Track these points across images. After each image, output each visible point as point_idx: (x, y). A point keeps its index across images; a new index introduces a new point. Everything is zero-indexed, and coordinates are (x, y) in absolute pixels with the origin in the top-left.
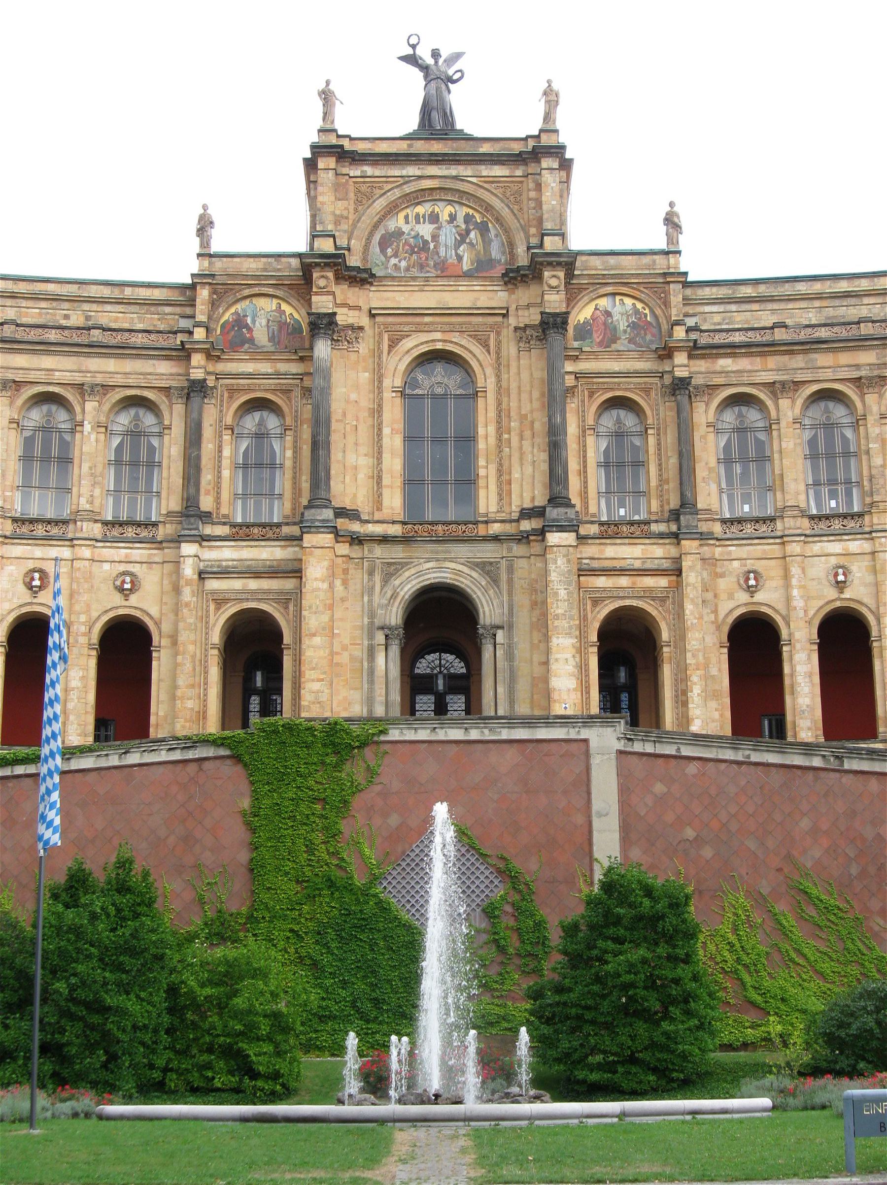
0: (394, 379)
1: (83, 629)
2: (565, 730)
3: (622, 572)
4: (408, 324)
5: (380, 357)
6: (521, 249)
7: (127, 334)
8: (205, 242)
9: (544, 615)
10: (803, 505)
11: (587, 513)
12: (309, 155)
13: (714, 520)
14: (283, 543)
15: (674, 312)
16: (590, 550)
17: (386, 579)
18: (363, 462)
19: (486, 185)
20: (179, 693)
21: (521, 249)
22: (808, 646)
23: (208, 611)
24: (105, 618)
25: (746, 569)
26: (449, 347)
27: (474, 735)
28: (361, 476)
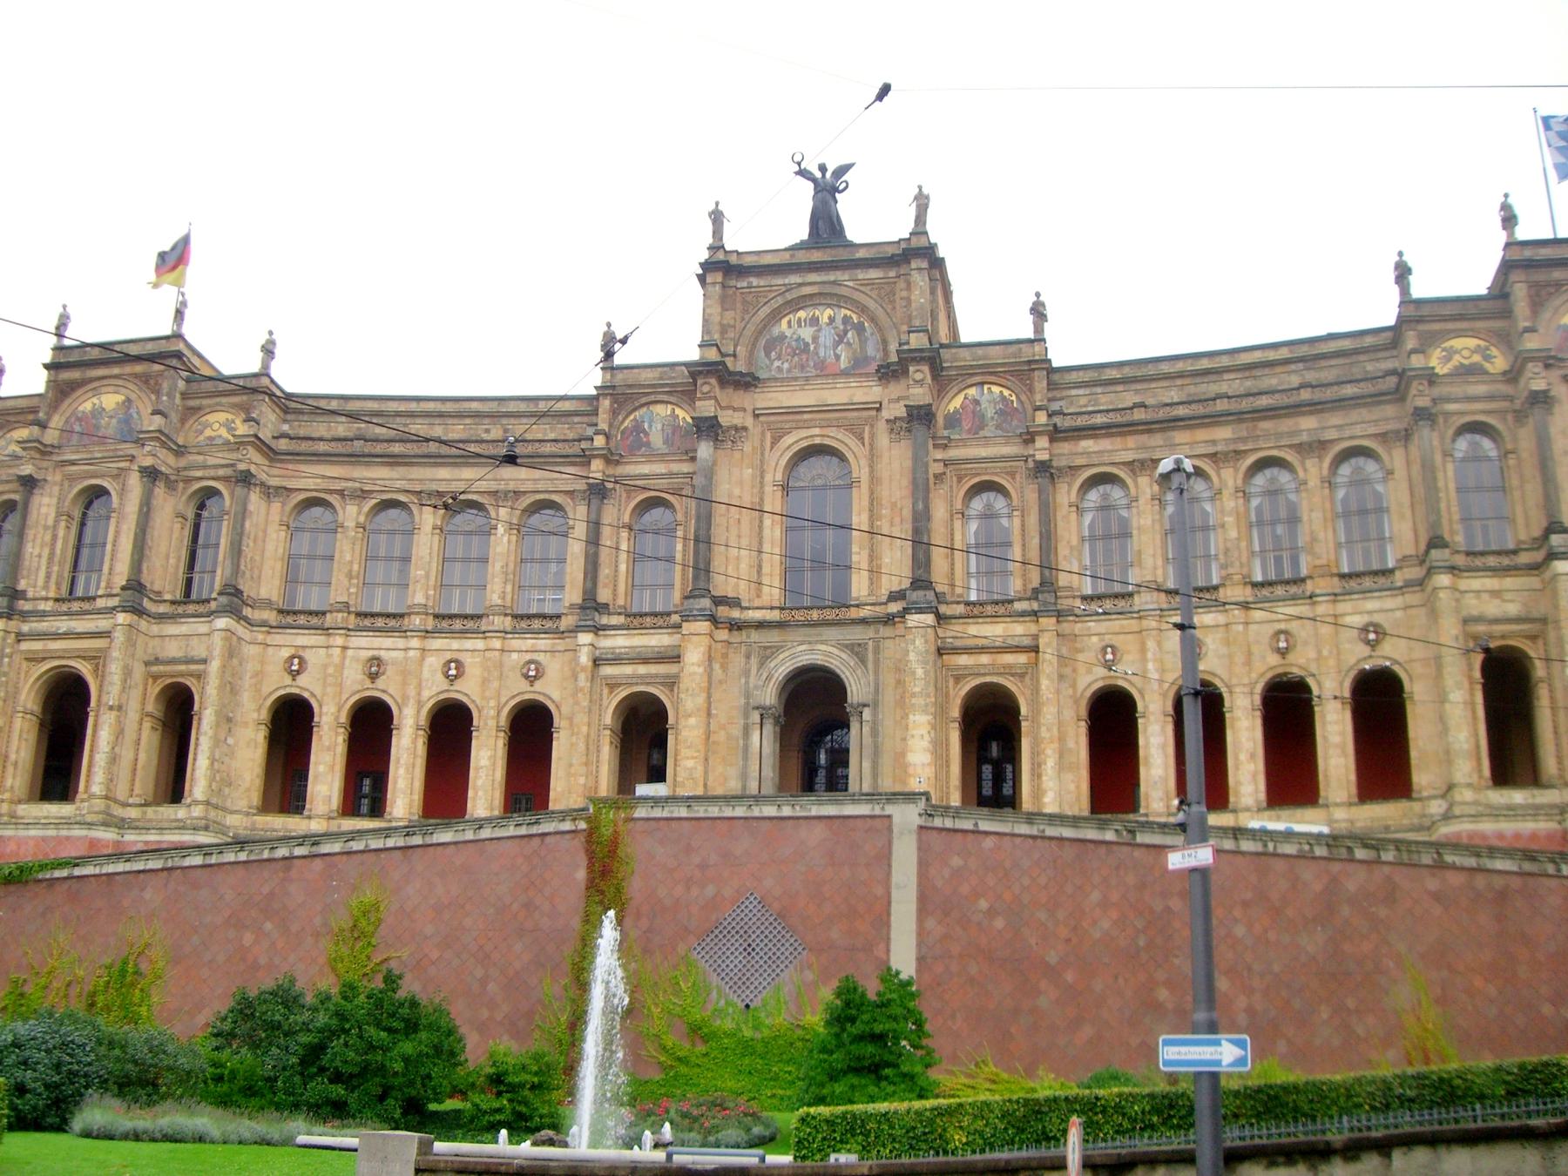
0: (775, 474)
1: (492, 713)
2: (870, 806)
3: (982, 650)
4: (786, 422)
5: (762, 454)
6: (893, 347)
7: (537, 444)
10: (1160, 580)
11: (953, 594)
12: (700, 271)
13: (1074, 597)
15: (1038, 397)
16: (956, 628)
19: (862, 288)
20: (573, 770)
21: (893, 347)
22: (1162, 718)
24: (513, 703)
25: (1104, 644)
26: (827, 442)
27: (787, 811)
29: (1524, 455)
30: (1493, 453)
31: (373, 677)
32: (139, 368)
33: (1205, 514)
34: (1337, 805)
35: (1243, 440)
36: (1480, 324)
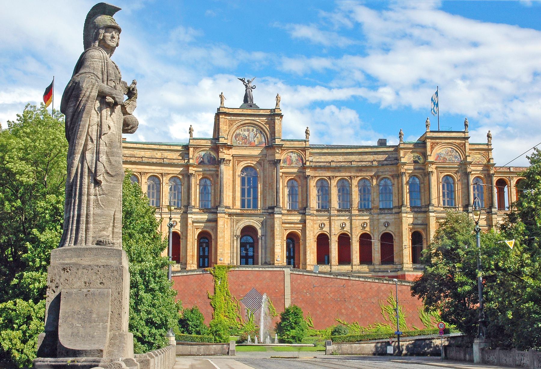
0: (238, 172)
8: (191, 136)
9: (274, 233)
14: (212, 214)
17: (237, 223)
18: (231, 194)
19: (261, 122)
23: (194, 231)
29: (426, 184)
30: (418, 183)
33: (347, 190)
34: (376, 265)
36: (418, 150)
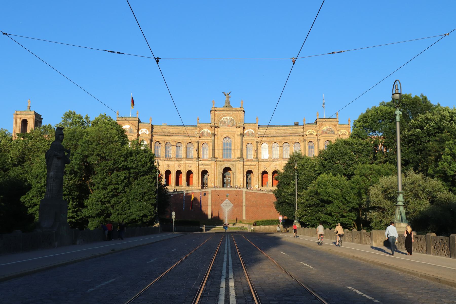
28: (218, 153)
31: (169, 167)
32: (132, 122)
35: (283, 140)
